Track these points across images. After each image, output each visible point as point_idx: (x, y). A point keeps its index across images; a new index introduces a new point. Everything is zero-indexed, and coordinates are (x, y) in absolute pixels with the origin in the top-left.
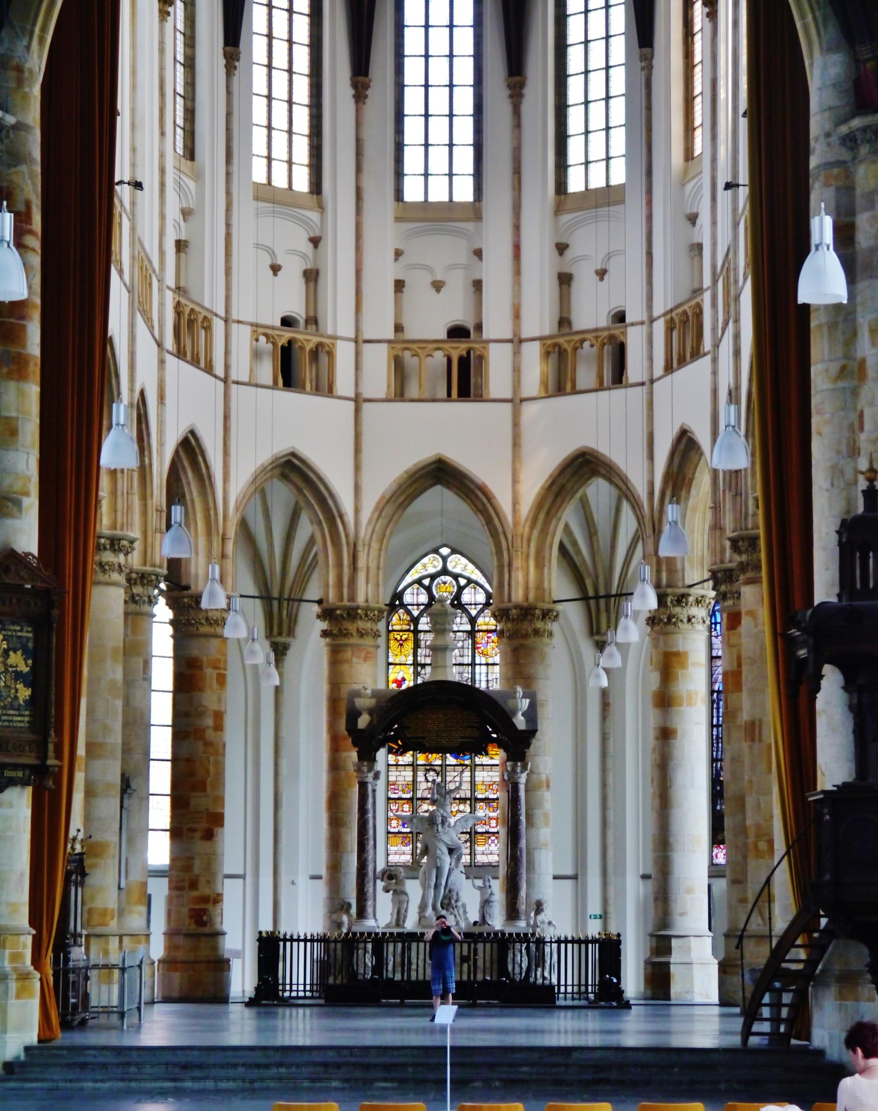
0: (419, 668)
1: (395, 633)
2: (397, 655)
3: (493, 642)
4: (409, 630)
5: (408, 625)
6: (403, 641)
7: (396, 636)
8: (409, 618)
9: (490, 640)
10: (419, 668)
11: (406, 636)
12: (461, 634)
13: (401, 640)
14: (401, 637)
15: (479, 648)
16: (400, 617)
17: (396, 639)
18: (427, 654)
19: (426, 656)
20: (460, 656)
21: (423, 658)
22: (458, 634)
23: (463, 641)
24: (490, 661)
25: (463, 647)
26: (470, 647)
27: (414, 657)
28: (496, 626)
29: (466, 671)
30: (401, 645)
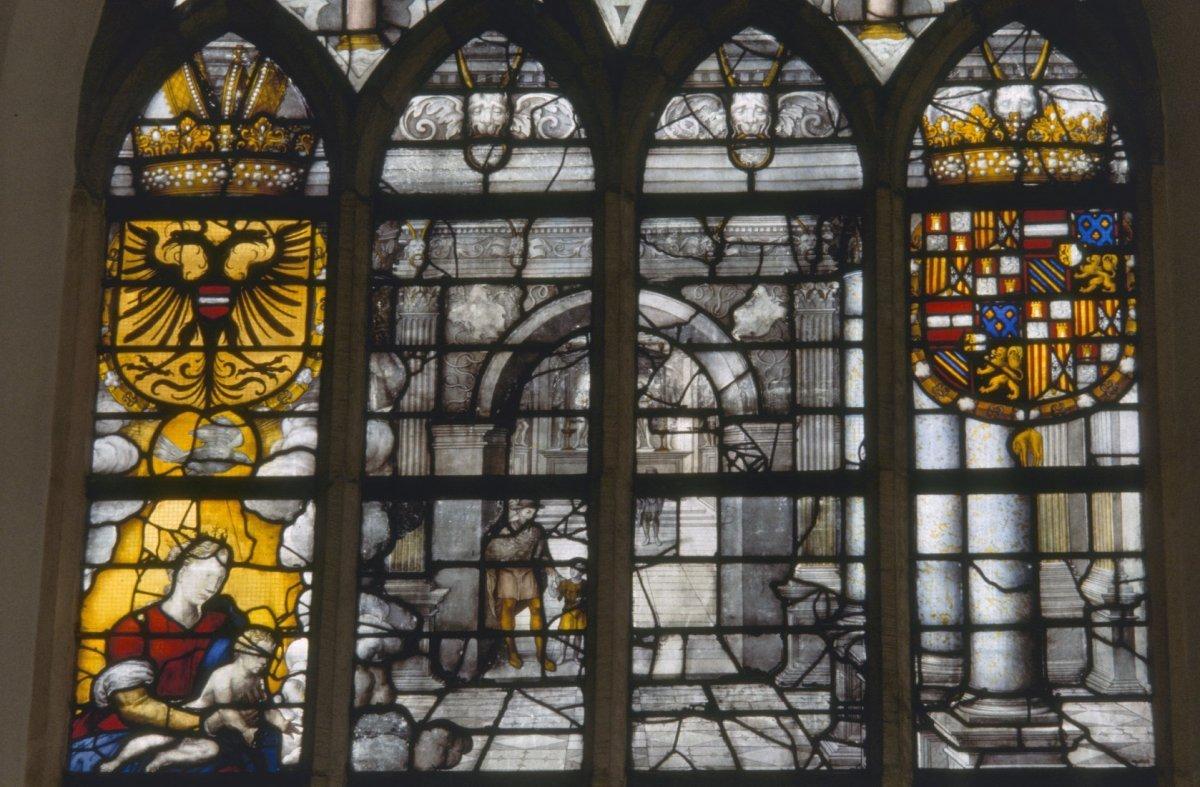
0: (375, 523)
1: (164, 229)
2: (166, 413)
3: (1073, 287)
4: (291, 203)
5: (285, 156)
6: (238, 290)
7: (166, 254)
8: (293, 103)
9: (1044, 276)
10: (375, 523)
11: (266, 251)
12: (771, 226)
13: (215, 276)
14: (217, 254)
15: (954, 339)
16: (207, 88)
17: (168, 277)
18: (457, 397)
19: (438, 416)
20: (761, 411)
21: (411, 431)
22: (744, 226)
23: (789, 284)
24: (1055, 447)
25: (788, 339)
26: (856, 331)
27: (322, 420)
28: (1106, 152)
29: (822, 543)
30: (214, 327)
